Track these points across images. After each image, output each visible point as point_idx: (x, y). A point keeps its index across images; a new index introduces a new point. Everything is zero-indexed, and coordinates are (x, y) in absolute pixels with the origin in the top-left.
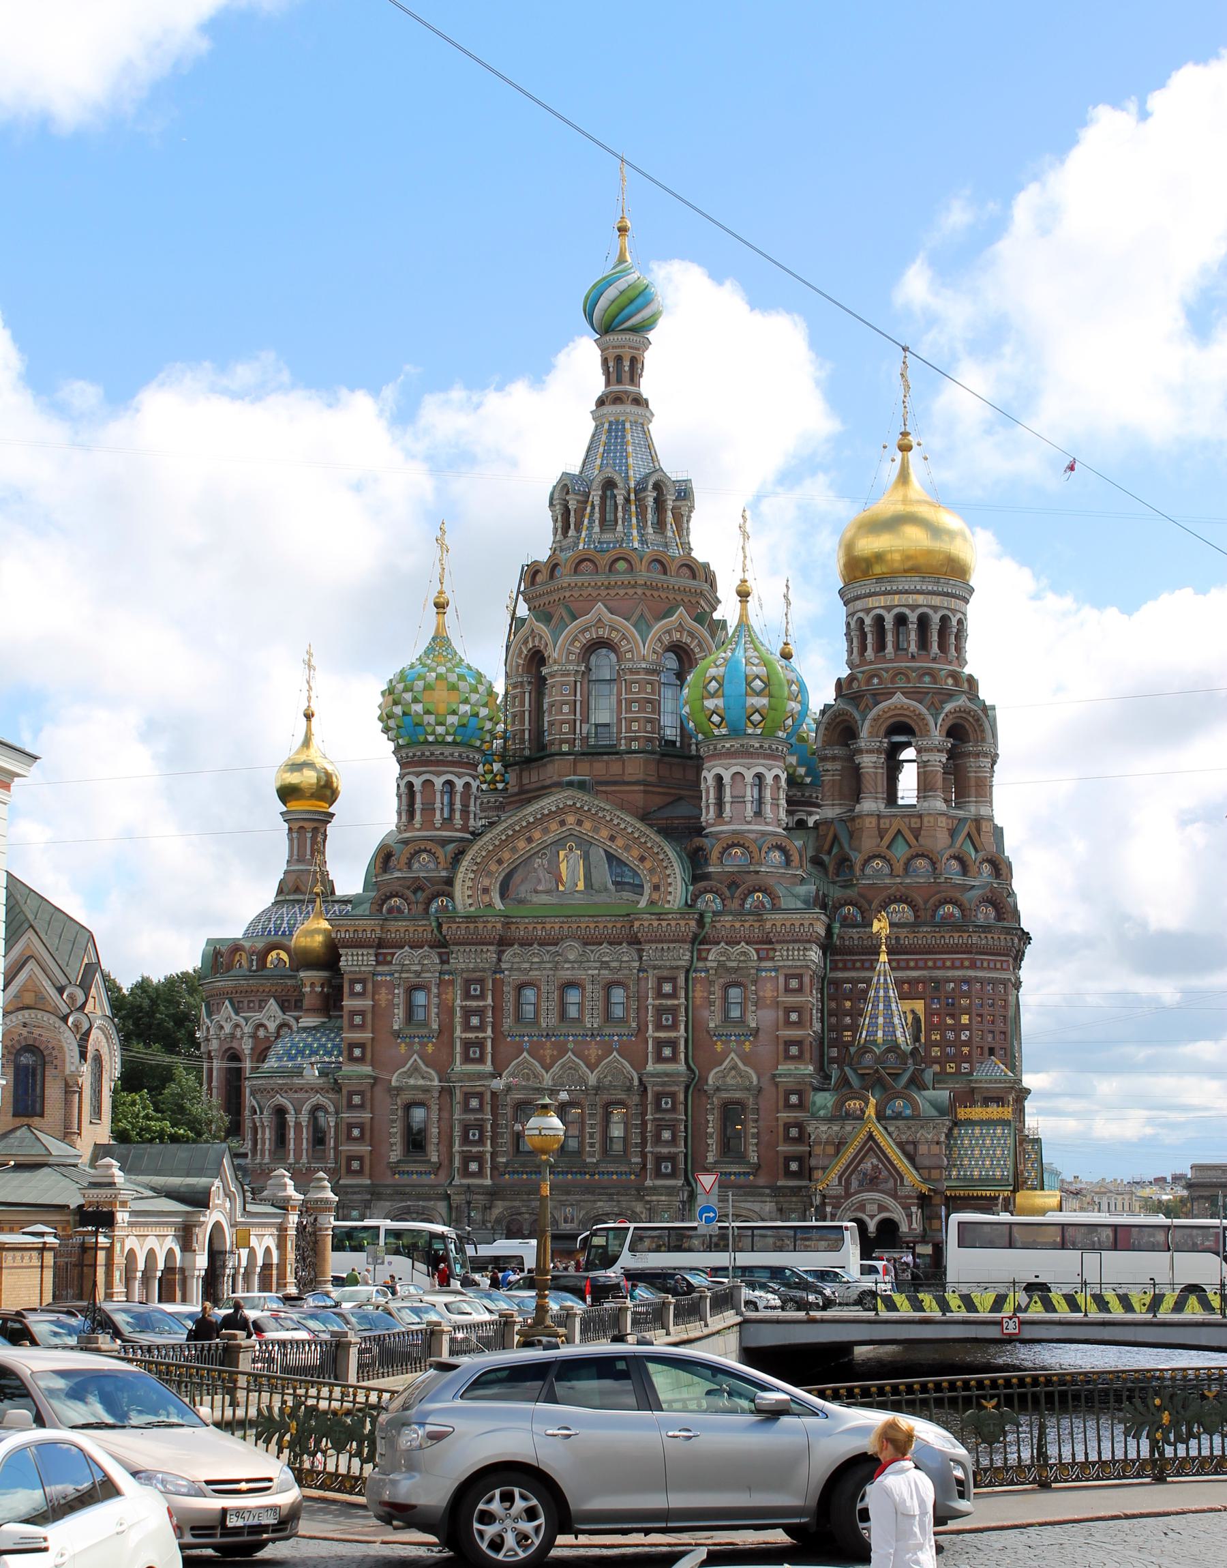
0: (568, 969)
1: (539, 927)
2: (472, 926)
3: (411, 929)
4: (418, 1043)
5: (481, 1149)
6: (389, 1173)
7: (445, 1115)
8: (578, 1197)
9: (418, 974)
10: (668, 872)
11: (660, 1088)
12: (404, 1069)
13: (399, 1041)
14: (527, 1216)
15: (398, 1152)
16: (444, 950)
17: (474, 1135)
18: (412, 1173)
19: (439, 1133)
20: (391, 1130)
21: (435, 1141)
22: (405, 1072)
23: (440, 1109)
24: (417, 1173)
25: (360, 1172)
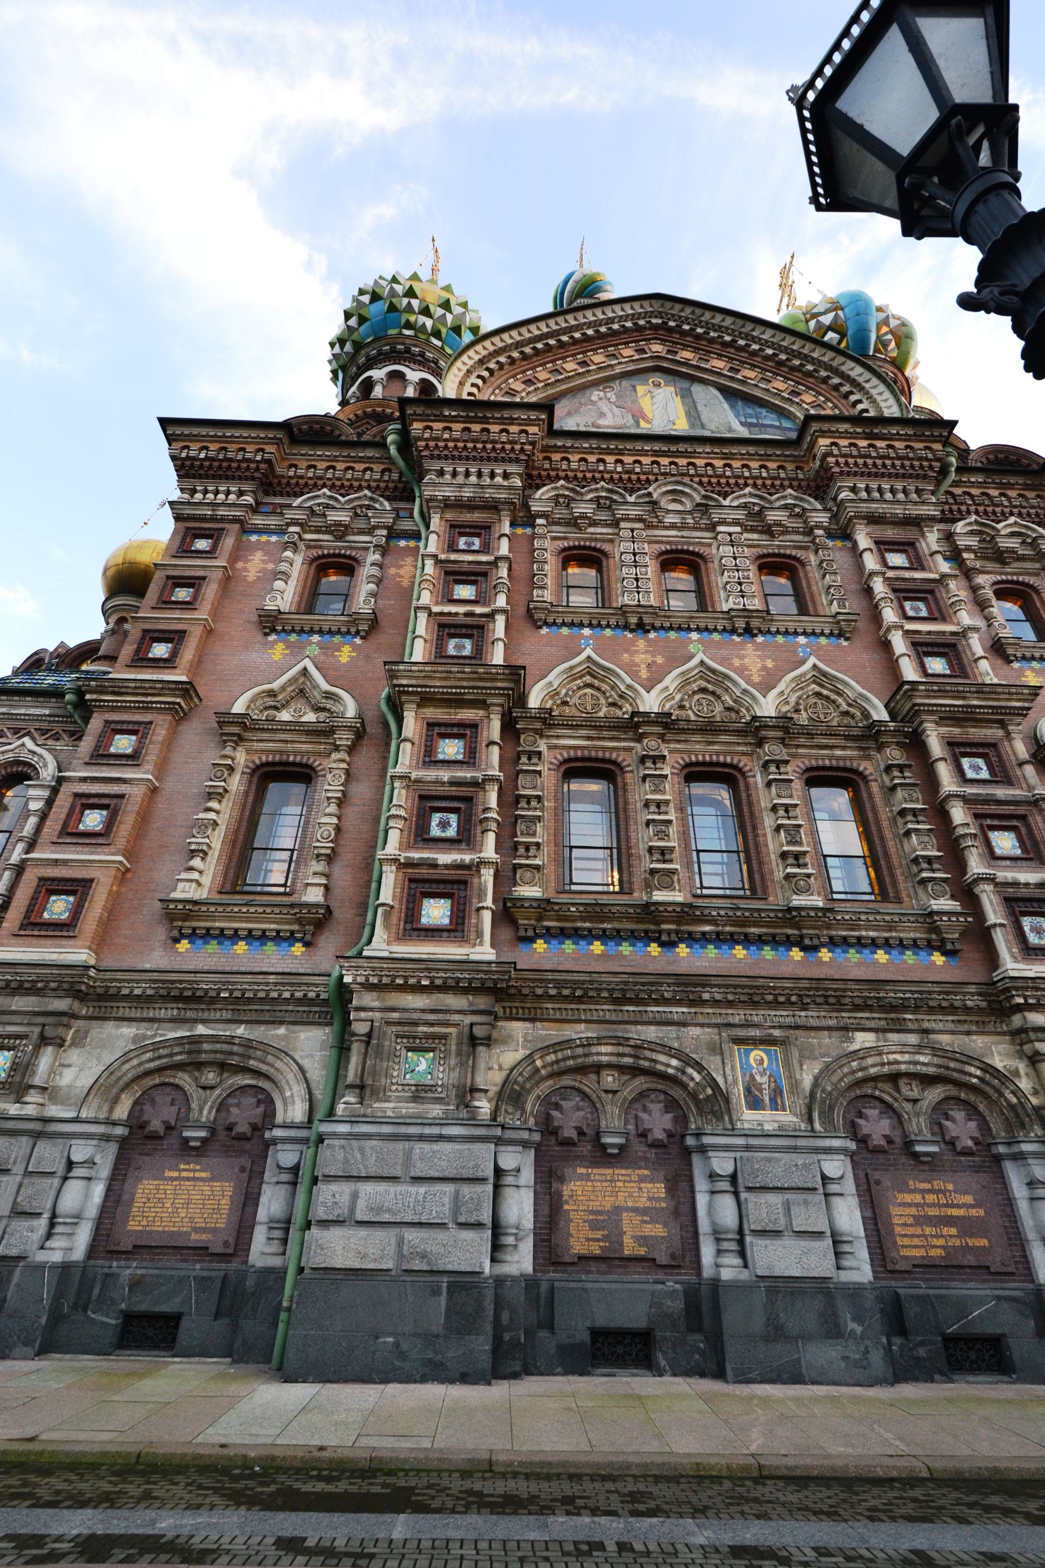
0: (673, 526)
1: (610, 459)
2: (476, 428)
3: (340, 466)
4: (318, 644)
5: (467, 858)
6: (161, 933)
7: (361, 790)
8: (783, 1016)
9: (340, 531)
10: (853, 398)
11: (957, 731)
12: (276, 685)
13: (272, 637)
14: (609, 1079)
15: (207, 880)
16: (402, 505)
17: (444, 825)
18: (235, 936)
19: (338, 829)
20: (201, 816)
21: (325, 846)
22: (272, 694)
23: (348, 772)
24: (249, 936)
25: (64, 929)
